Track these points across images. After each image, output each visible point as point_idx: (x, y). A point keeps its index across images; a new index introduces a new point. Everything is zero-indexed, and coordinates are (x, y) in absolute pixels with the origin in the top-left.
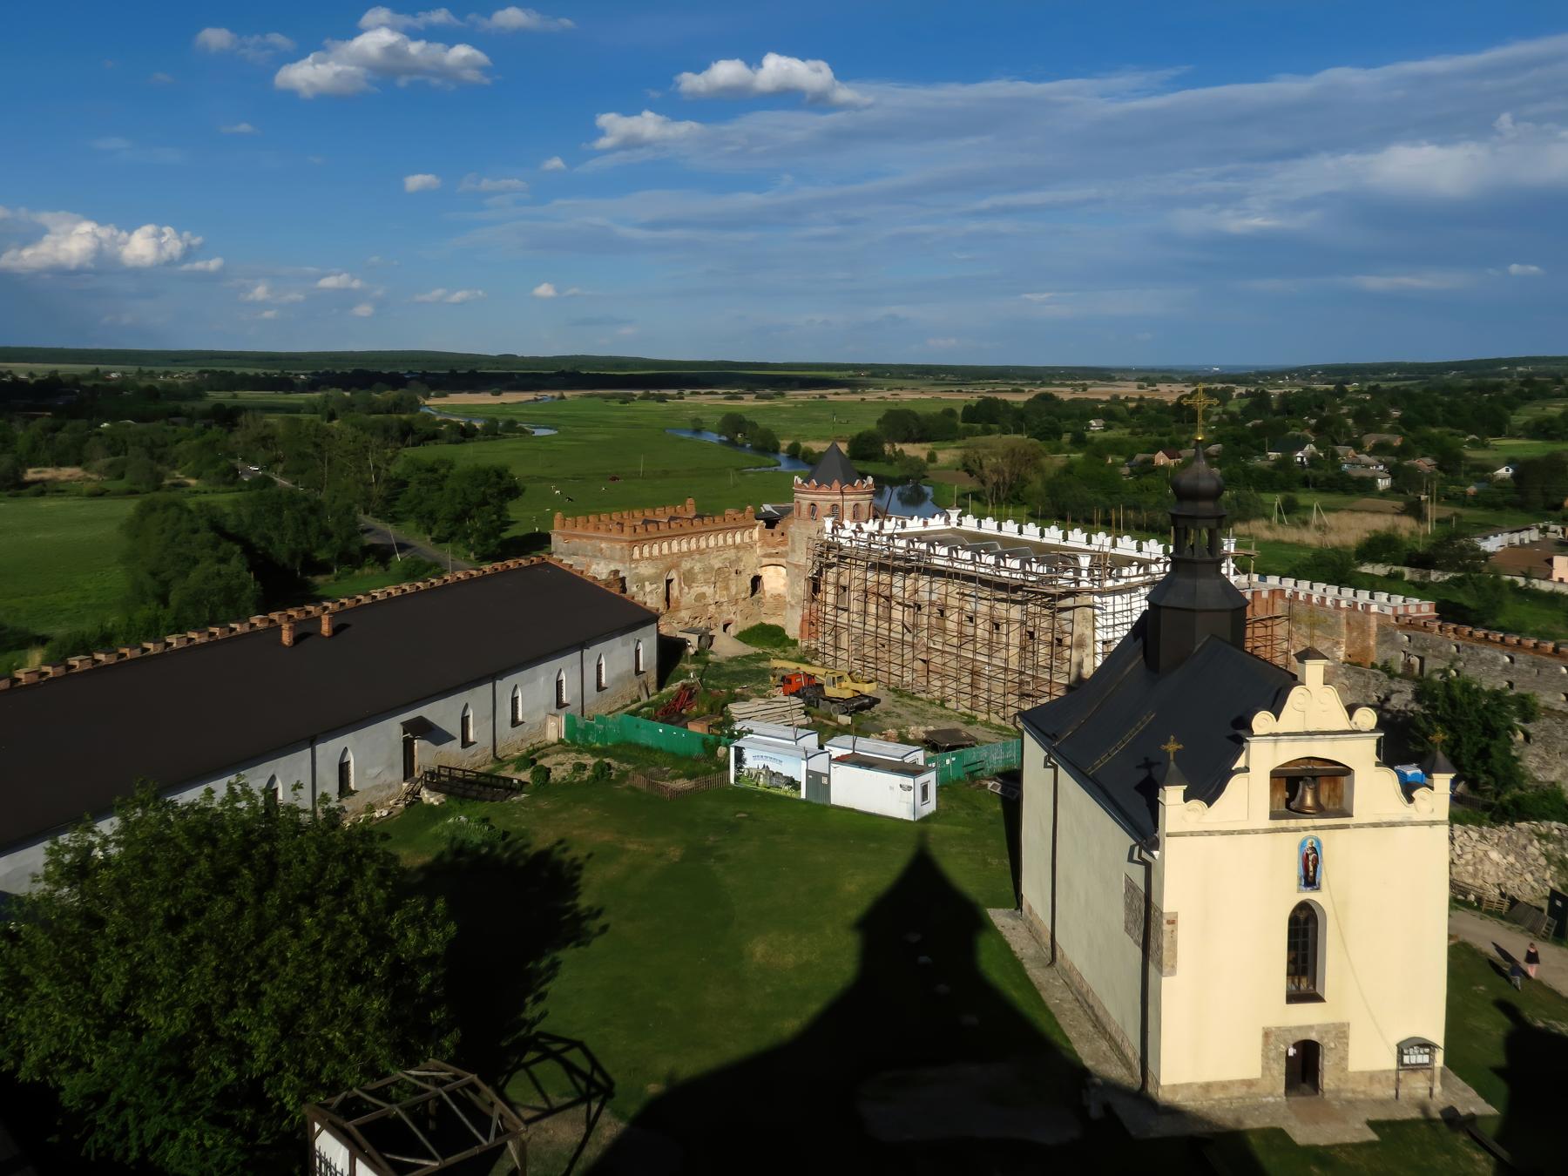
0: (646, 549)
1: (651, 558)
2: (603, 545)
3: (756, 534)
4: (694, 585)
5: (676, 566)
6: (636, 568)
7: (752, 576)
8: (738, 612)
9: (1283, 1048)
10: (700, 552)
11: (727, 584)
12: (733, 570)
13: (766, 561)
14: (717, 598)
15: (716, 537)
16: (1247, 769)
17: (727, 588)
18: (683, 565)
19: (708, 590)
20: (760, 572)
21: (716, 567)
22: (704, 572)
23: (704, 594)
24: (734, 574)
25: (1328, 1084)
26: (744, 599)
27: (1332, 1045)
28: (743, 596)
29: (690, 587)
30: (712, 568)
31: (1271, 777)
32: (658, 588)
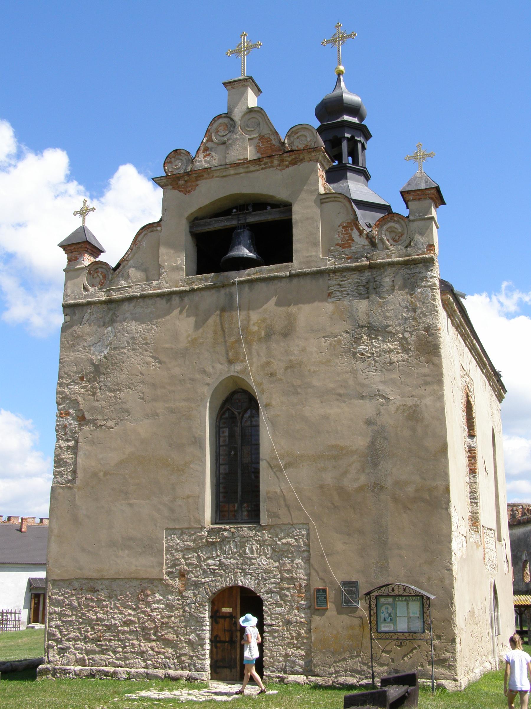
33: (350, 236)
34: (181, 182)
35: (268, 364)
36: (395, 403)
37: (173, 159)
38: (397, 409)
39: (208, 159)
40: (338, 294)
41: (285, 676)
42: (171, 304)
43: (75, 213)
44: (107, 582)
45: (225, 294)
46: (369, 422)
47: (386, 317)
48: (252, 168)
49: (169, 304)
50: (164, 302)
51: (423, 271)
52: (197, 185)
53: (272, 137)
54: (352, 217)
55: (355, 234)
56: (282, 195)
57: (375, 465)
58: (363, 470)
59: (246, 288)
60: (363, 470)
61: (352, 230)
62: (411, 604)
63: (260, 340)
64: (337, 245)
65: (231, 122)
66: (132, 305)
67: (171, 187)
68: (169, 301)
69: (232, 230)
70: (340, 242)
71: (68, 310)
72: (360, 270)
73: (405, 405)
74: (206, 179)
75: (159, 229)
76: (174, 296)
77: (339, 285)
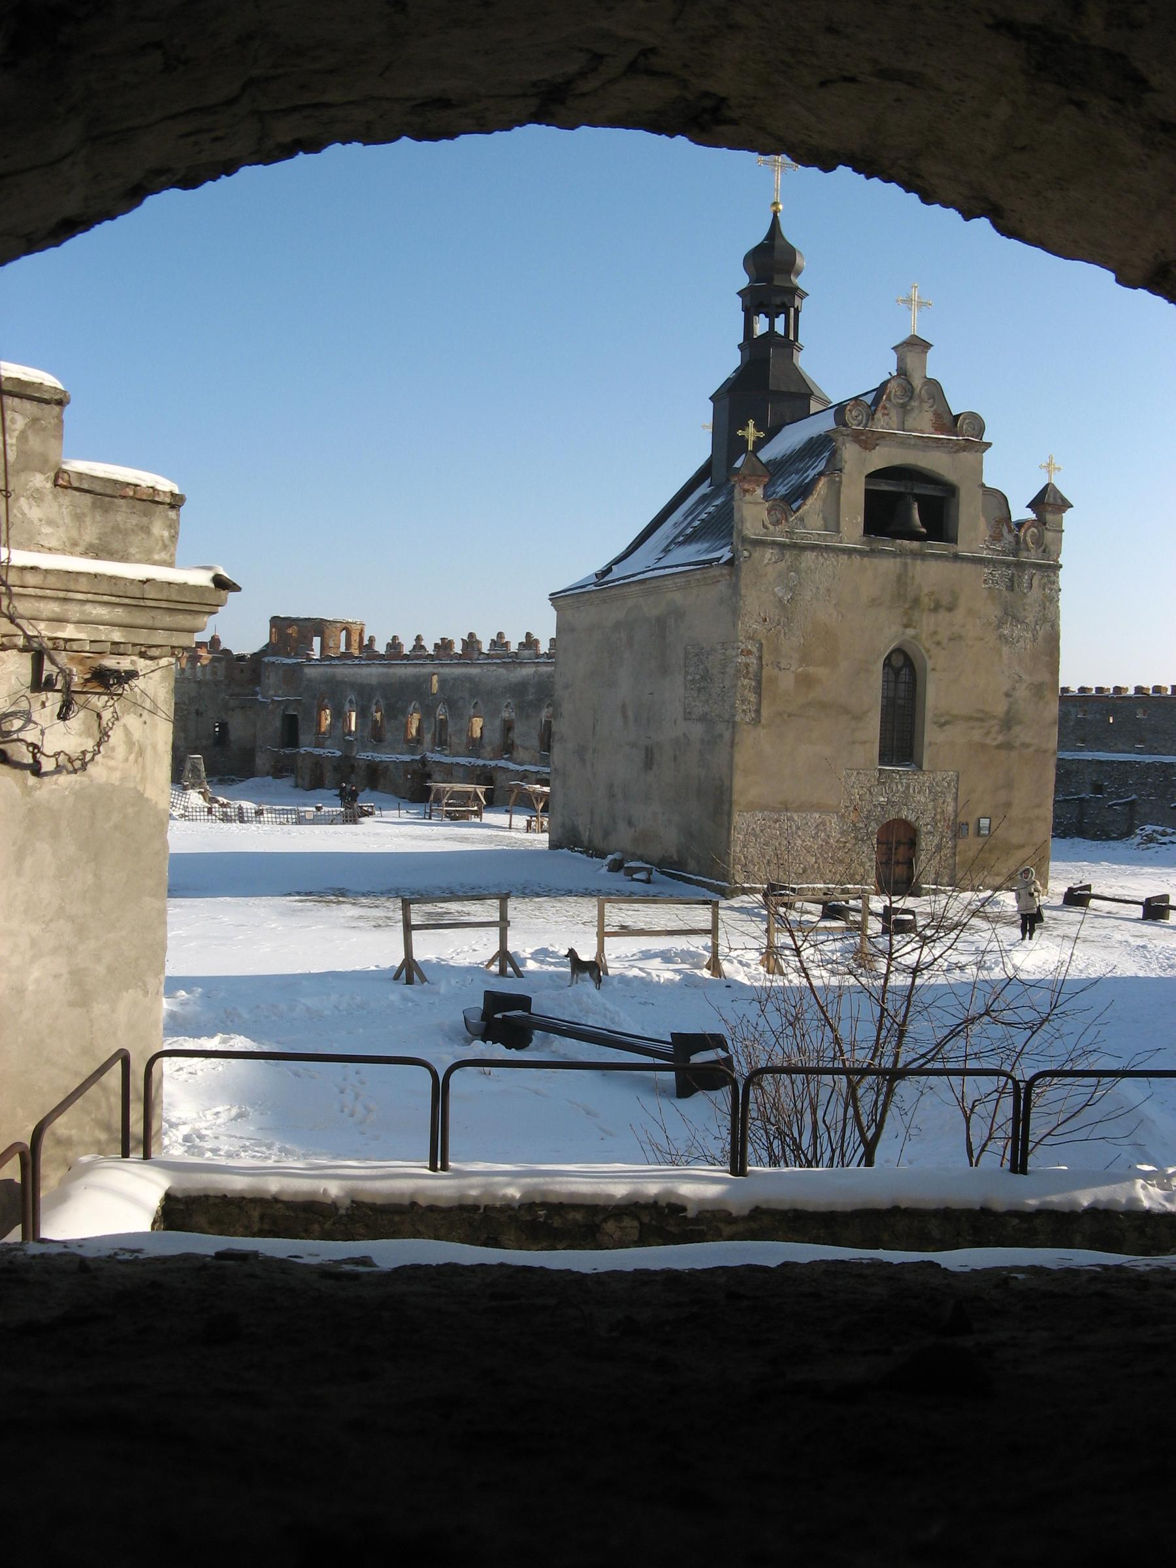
9: (874, 827)
13: (233, 703)
28: (204, 742)
33: (1001, 531)
35: (935, 633)
36: (1025, 682)
38: (1027, 687)
39: (886, 417)
46: (1007, 695)
47: (1025, 610)
50: (846, 557)
51: (1052, 574)
55: (1005, 530)
56: (951, 476)
57: (1009, 729)
58: (1000, 732)
60: (1000, 732)
61: (1003, 525)
63: (930, 610)
65: (909, 386)
67: (851, 439)
69: (899, 496)
72: (1008, 565)
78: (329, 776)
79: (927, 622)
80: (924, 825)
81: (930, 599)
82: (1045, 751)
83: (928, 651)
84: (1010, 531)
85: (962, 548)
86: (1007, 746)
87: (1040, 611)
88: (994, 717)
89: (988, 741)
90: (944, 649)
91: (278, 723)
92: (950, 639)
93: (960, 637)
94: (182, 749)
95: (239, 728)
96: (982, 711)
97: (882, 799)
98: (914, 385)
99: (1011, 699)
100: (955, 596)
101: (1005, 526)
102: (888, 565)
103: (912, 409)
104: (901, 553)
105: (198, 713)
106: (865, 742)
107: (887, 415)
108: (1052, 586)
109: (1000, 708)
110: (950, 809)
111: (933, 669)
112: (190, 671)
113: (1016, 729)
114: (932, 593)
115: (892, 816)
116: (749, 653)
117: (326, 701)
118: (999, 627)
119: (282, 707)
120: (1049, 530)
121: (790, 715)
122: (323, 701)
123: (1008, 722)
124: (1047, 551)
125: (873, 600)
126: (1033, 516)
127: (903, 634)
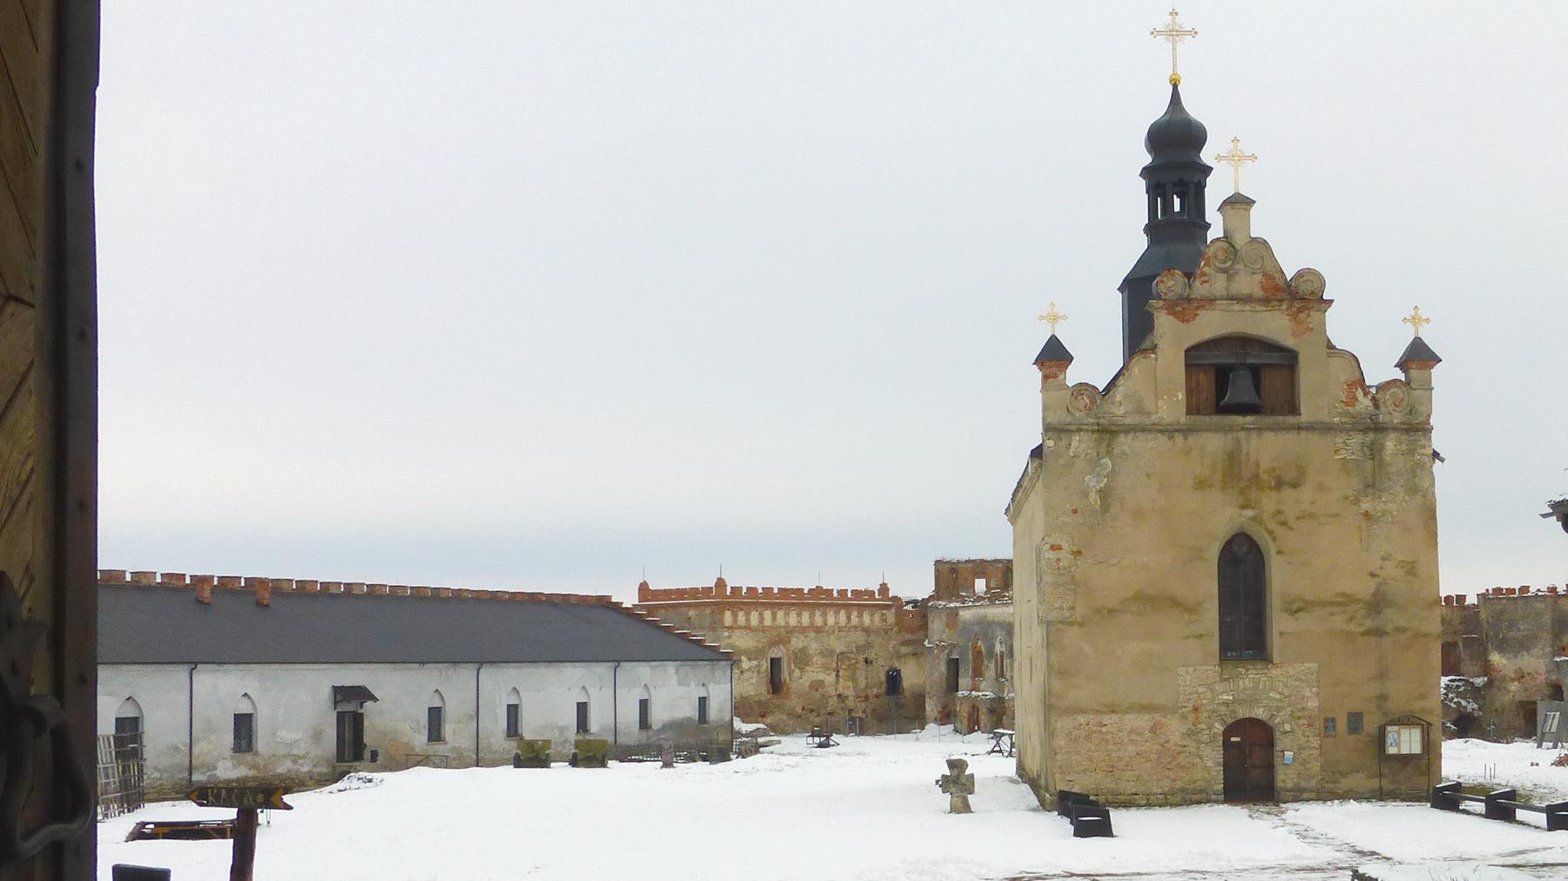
0: (741, 616)
1: (748, 628)
2: (692, 613)
3: (891, 617)
4: (808, 668)
5: (786, 642)
6: (729, 637)
7: (886, 668)
8: (868, 711)
9: (1219, 728)
10: (818, 630)
11: (854, 674)
12: (861, 658)
13: (904, 650)
14: (840, 690)
15: (837, 614)
16: (1155, 347)
17: (853, 678)
18: (793, 642)
19: (829, 679)
20: (897, 665)
21: (838, 651)
22: (822, 653)
23: (821, 682)
24: (862, 664)
25: (1283, 781)
26: (877, 696)
27: (1287, 727)
28: (875, 691)
29: (802, 670)
30: (832, 652)
31: (1189, 366)
32: (759, 665)
33: (1355, 395)
34: (1179, 309)
35: (1280, 512)
37: (1165, 278)
39: (1206, 285)
40: (1344, 452)
41: (1299, 794)
42: (1174, 441)
43: (1041, 318)
44: (1115, 717)
45: (1233, 438)
46: (1373, 575)
47: (1389, 479)
48: (1258, 308)
49: (1172, 441)
52: (1197, 315)
53: (1277, 276)
54: (1358, 376)
55: (1360, 394)
56: (1289, 342)
57: (1379, 613)
59: (1254, 435)
61: (1357, 389)
62: (1413, 731)
63: (1270, 488)
64: (1342, 402)
66: (1131, 436)
67: (1166, 311)
68: (1171, 438)
70: (1344, 400)
71: (1050, 434)
73: (1403, 561)
74: (1207, 310)
75: (1153, 356)
76: (1177, 433)
77: (1344, 442)
78: (984, 718)
79: (1269, 501)
80: (1282, 723)
81: (1270, 476)
82: (1427, 635)
83: (1271, 532)
84: (1366, 394)
85: (1305, 416)
86: (1378, 632)
87: (1408, 480)
88: (1358, 601)
89: (1352, 627)
90: (1291, 529)
91: (943, 668)
92: (1298, 518)
93: (1312, 515)
94: (850, 698)
95: (911, 676)
96: (1343, 595)
97: (1225, 697)
98: (1238, 247)
99: (1378, 580)
100: (1301, 471)
101: (1360, 390)
102: (1213, 443)
103: (1237, 273)
104: (1230, 429)
105: (866, 661)
106: (1202, 636)
107: (1206, 282)
108: (1423, 451)
109: (1363, 588)
110: (1313, 704)
111: (1279, 552)
112: (857, 619)
113: (1389, 613)
114: (1274, 469)
115: (1243, 713)
116: (1059, 548)
117: (980, 643)
118: (1357, 501)
119: (946, 651)
120: (1415, 389)
121: (1110, 611)
122: (977, 643)
123: (1377, 604)
124: (1413, 411)
125: (1201, 482)
126: (1402, 377)
127: (1240, 515)
